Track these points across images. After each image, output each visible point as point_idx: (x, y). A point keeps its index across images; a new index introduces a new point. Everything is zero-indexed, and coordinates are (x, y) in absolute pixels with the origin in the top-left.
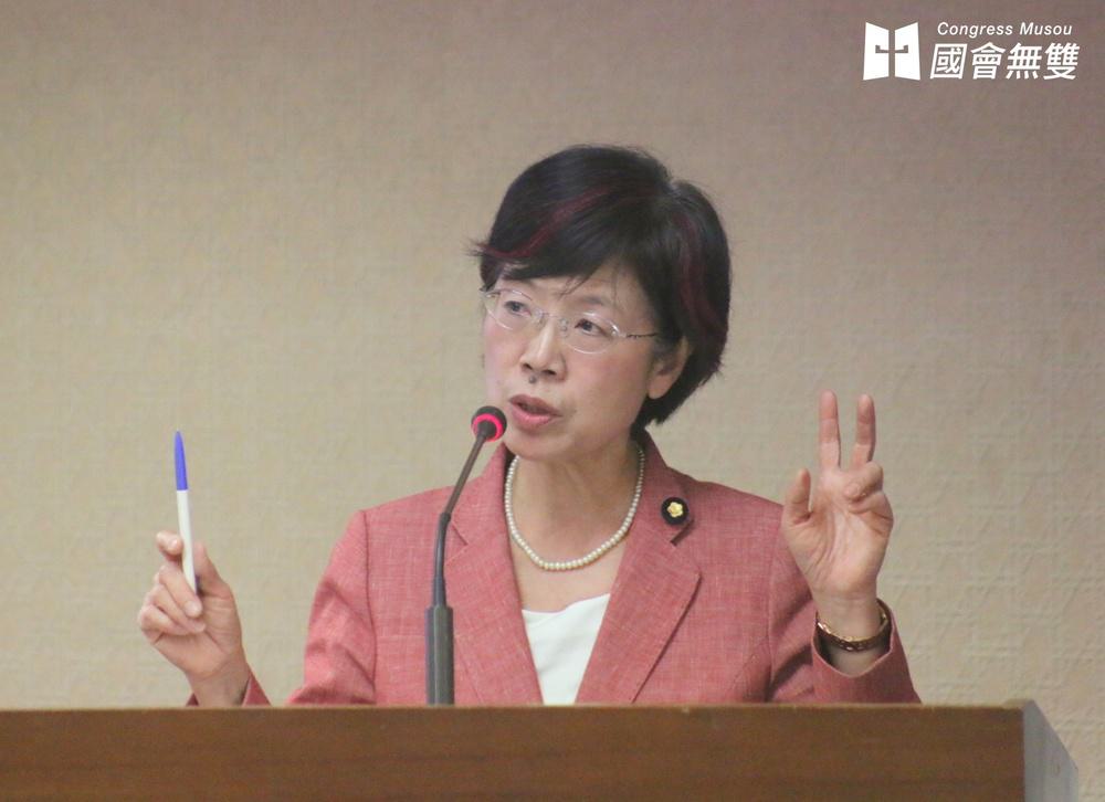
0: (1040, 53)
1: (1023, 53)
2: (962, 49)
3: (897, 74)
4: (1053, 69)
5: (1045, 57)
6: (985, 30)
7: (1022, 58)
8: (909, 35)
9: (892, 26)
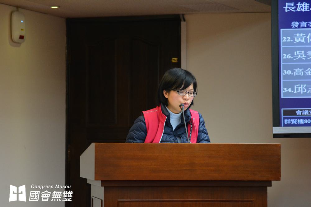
0: (61, 194)
1: (56, 194)
2: (38, 192)
3: (19, 200)
4: (65, 198)
5: (63, 195)
6: (45, 187)
7: (56, 195)
8: (23, 188)
9: (18, 186)
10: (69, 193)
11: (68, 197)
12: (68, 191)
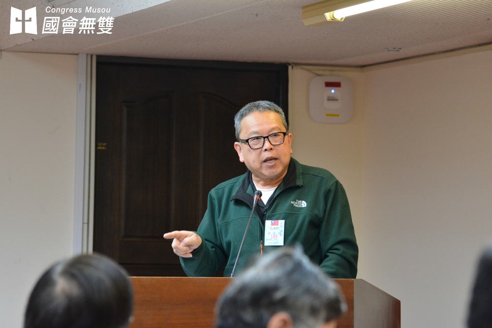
1: (87, 21)
2: (57, 19)
3: (27, 31)
4: (101, 29)
5: (98, 24)
6: (68, 10)
7: (86, 24)
8: (31, 13)
9: (23, 8)
10: (107, 20)
11: (105, 27)
12: (106, 18)
